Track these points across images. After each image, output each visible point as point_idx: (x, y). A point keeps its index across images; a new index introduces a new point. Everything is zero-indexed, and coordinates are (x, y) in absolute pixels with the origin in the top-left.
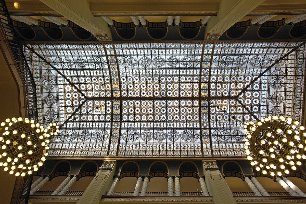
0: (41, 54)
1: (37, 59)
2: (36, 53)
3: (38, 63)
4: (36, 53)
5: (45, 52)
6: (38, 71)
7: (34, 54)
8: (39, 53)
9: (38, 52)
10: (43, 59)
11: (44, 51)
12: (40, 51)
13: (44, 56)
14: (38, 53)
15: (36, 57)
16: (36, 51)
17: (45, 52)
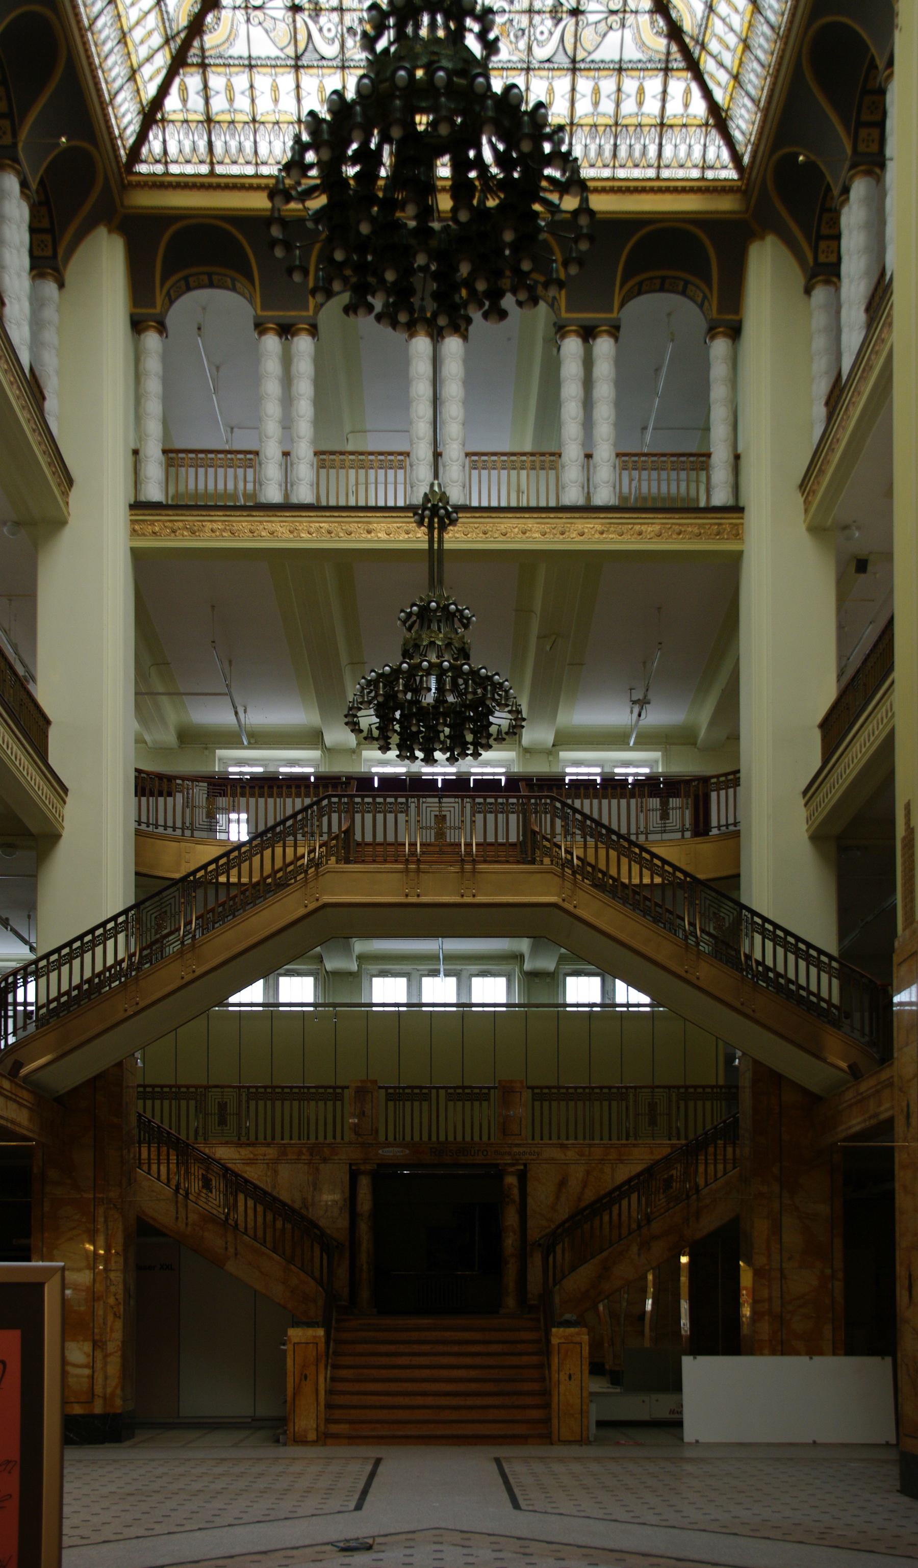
0: (162, 60)
1: (193, 81)
2: (164, 90)
3: (216, 81)
4: (164, 90)
5: (142, 42)
6: (263, 81)
7: (172, 103)
8: (158, 71)
9: (151, 79)
10: (186, 45)
11: (143, 52)
12: (147, 71)
13: (167, 41)
14: (159, 80)
15: (184, 90)
16: (151, 90)
17: (142, 42)
